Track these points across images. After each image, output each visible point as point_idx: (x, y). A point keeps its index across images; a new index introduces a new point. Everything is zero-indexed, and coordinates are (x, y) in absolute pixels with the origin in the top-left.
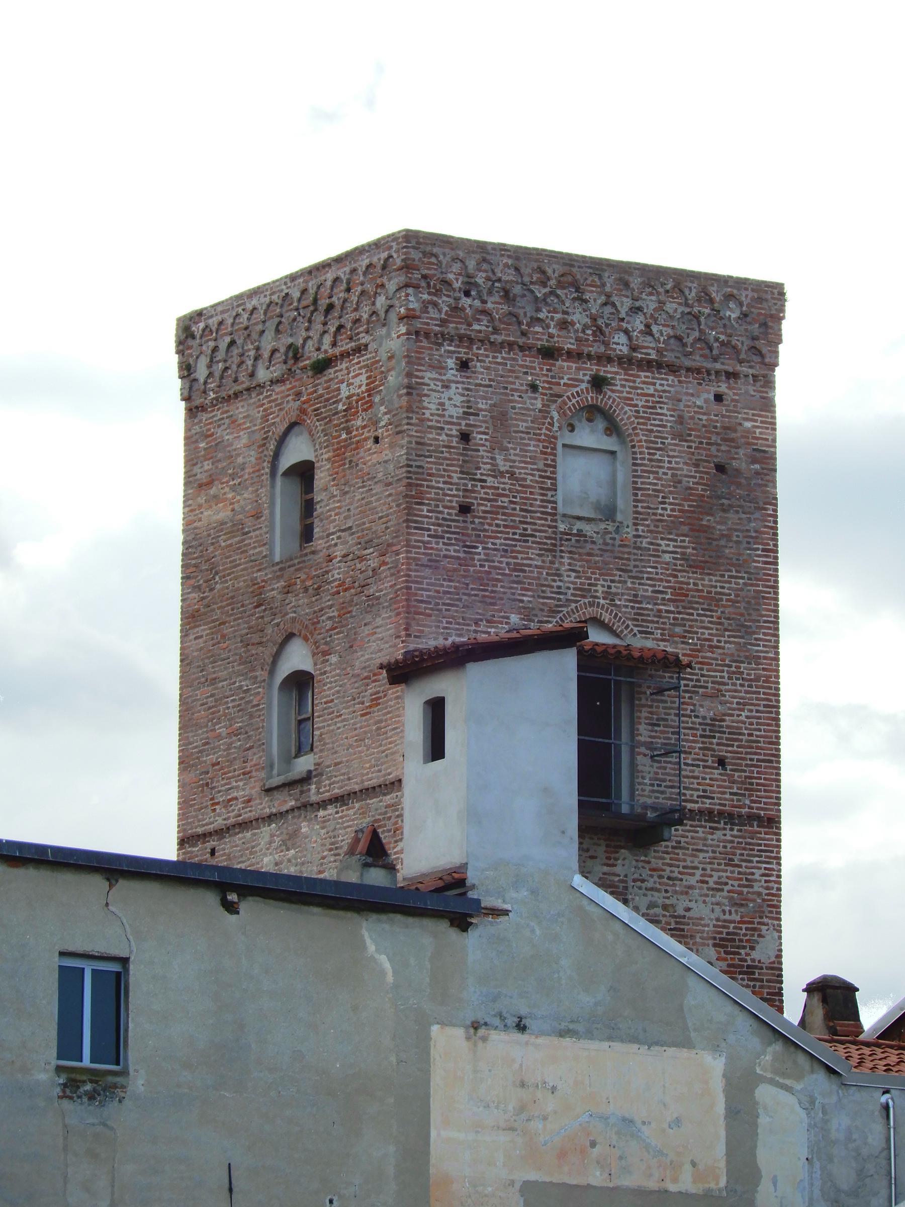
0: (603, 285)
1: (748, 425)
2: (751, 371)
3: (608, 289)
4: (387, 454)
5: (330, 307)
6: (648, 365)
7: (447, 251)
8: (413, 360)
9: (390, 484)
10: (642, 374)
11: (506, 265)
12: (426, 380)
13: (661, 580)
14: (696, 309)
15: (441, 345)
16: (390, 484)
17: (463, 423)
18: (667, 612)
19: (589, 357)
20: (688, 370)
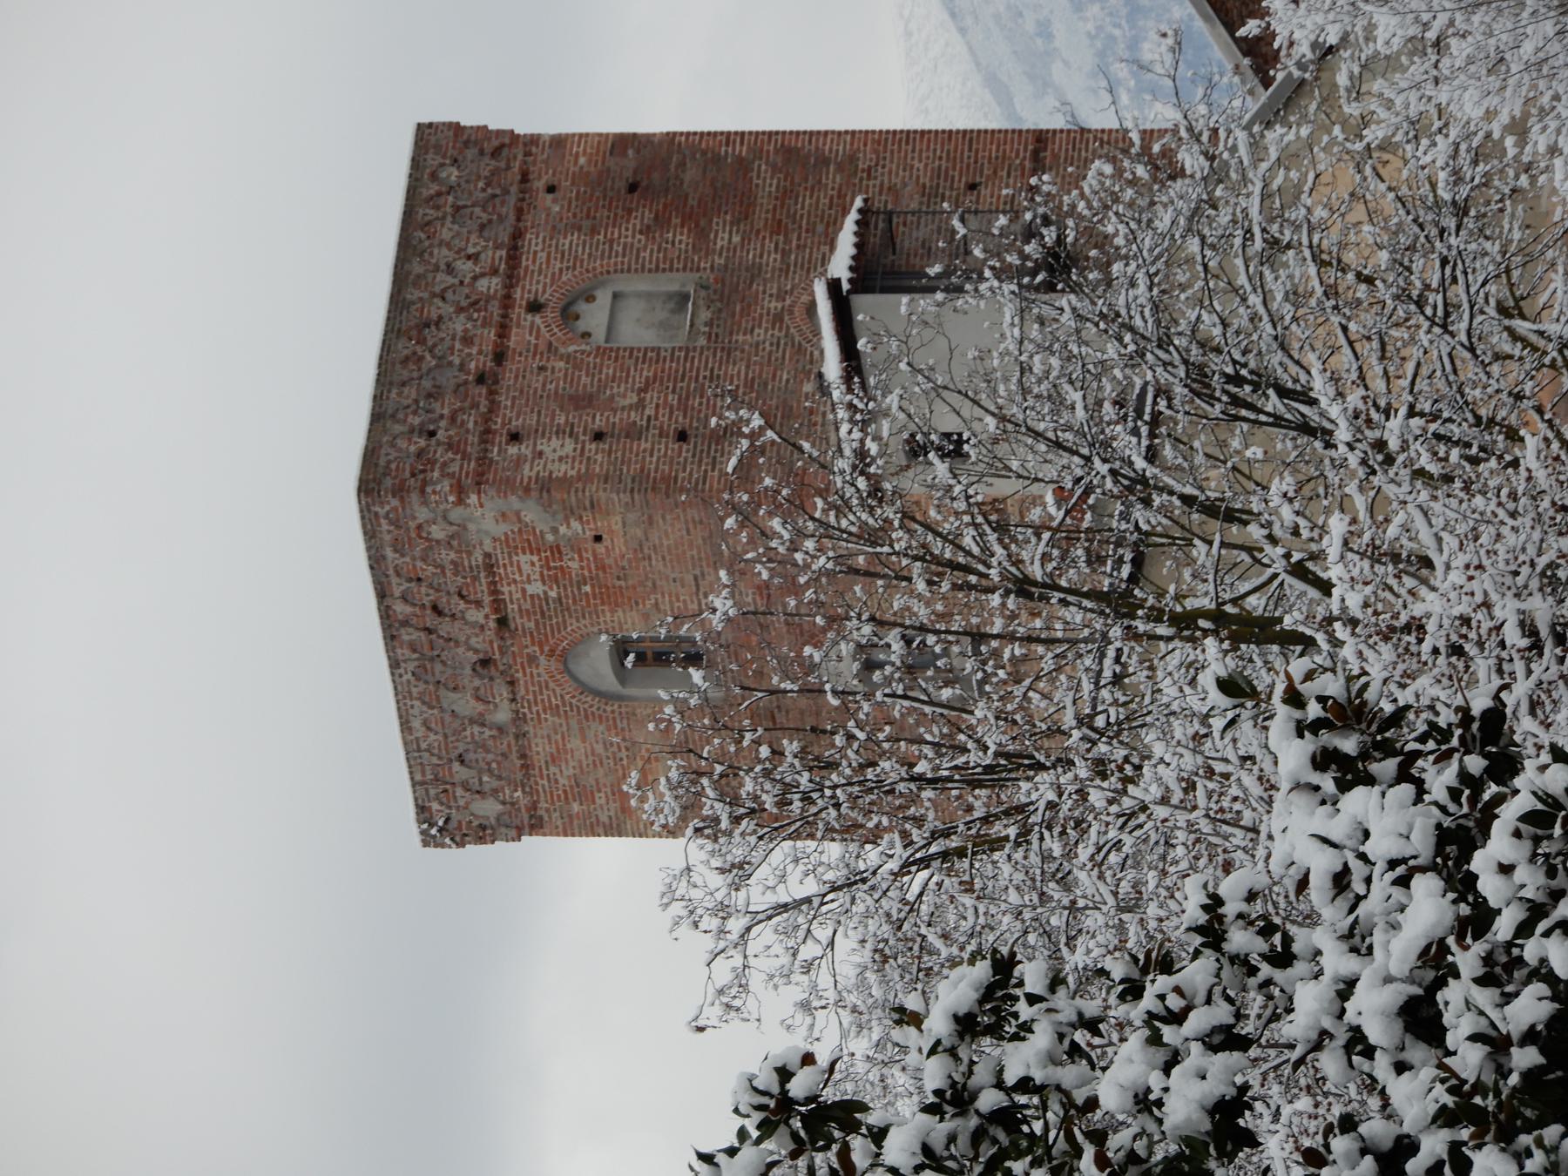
0: (421, 299)
1: (582, 160)
2: (520, 157)
3: (425, 295)
4: (616, 522)
5: (436, 609)
6: (514, 258)
7: (383, 451)
8: (507, 486)
9: (650, 517)
10: (524, 263)
11: (400, 394)
12: (533, 474)
13: (763, 245)
14: (449, 209)
15: (491, 460)
16: (650, 517)
17: (582, 438)
18: (799, 238)
19: (505, 316)
20: (519, 220)
